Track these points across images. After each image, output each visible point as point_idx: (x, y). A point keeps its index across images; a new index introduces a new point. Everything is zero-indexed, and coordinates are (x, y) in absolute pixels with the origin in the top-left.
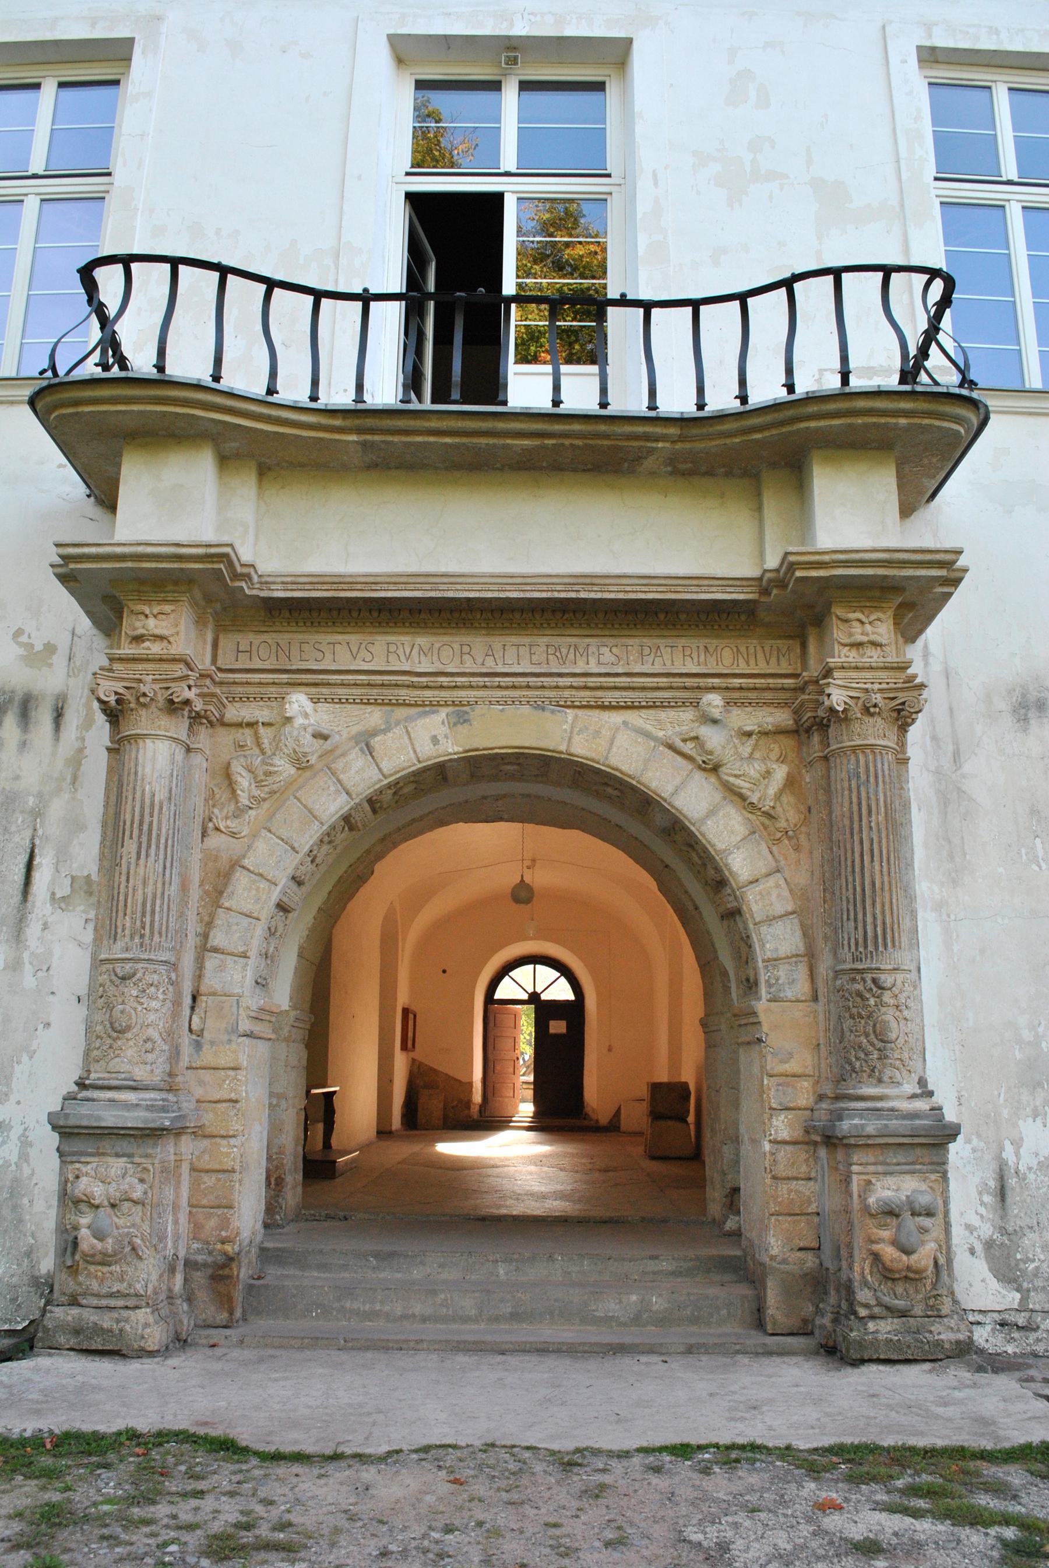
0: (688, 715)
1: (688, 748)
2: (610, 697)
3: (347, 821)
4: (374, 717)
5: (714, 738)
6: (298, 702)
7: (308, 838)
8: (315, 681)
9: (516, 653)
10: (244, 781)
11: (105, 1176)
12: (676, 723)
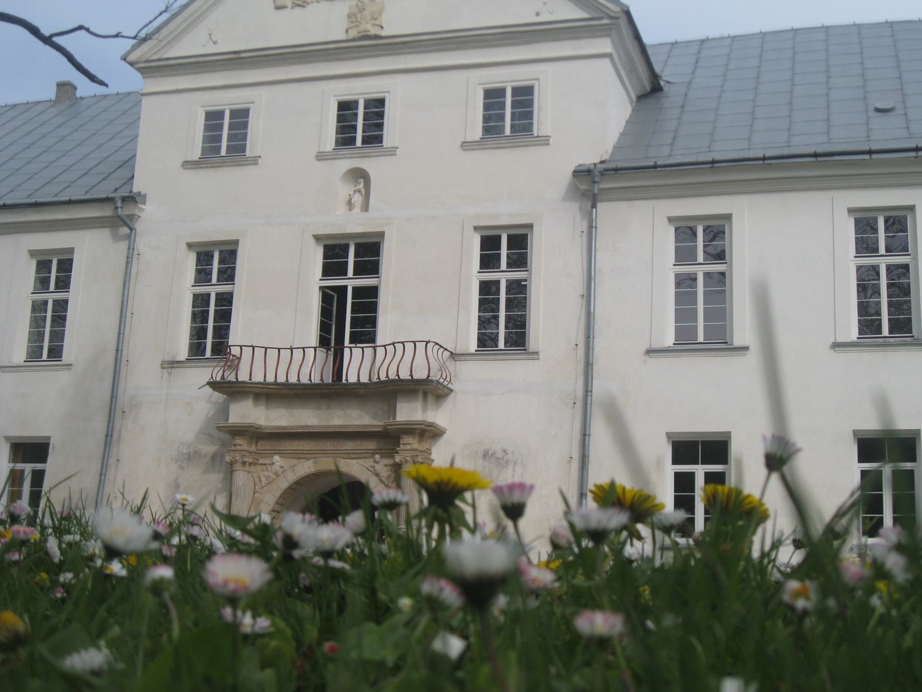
0: (372, 460)
1: (372, 469)
2: (353, 456)
3: (290, 488)
4: (295, 461)
5: (377, 467)
6: (277, 458)
7: (278, 494)
8: (281, 453)
9: (328, 445)
10: (263, 479)
12: (369, 462)
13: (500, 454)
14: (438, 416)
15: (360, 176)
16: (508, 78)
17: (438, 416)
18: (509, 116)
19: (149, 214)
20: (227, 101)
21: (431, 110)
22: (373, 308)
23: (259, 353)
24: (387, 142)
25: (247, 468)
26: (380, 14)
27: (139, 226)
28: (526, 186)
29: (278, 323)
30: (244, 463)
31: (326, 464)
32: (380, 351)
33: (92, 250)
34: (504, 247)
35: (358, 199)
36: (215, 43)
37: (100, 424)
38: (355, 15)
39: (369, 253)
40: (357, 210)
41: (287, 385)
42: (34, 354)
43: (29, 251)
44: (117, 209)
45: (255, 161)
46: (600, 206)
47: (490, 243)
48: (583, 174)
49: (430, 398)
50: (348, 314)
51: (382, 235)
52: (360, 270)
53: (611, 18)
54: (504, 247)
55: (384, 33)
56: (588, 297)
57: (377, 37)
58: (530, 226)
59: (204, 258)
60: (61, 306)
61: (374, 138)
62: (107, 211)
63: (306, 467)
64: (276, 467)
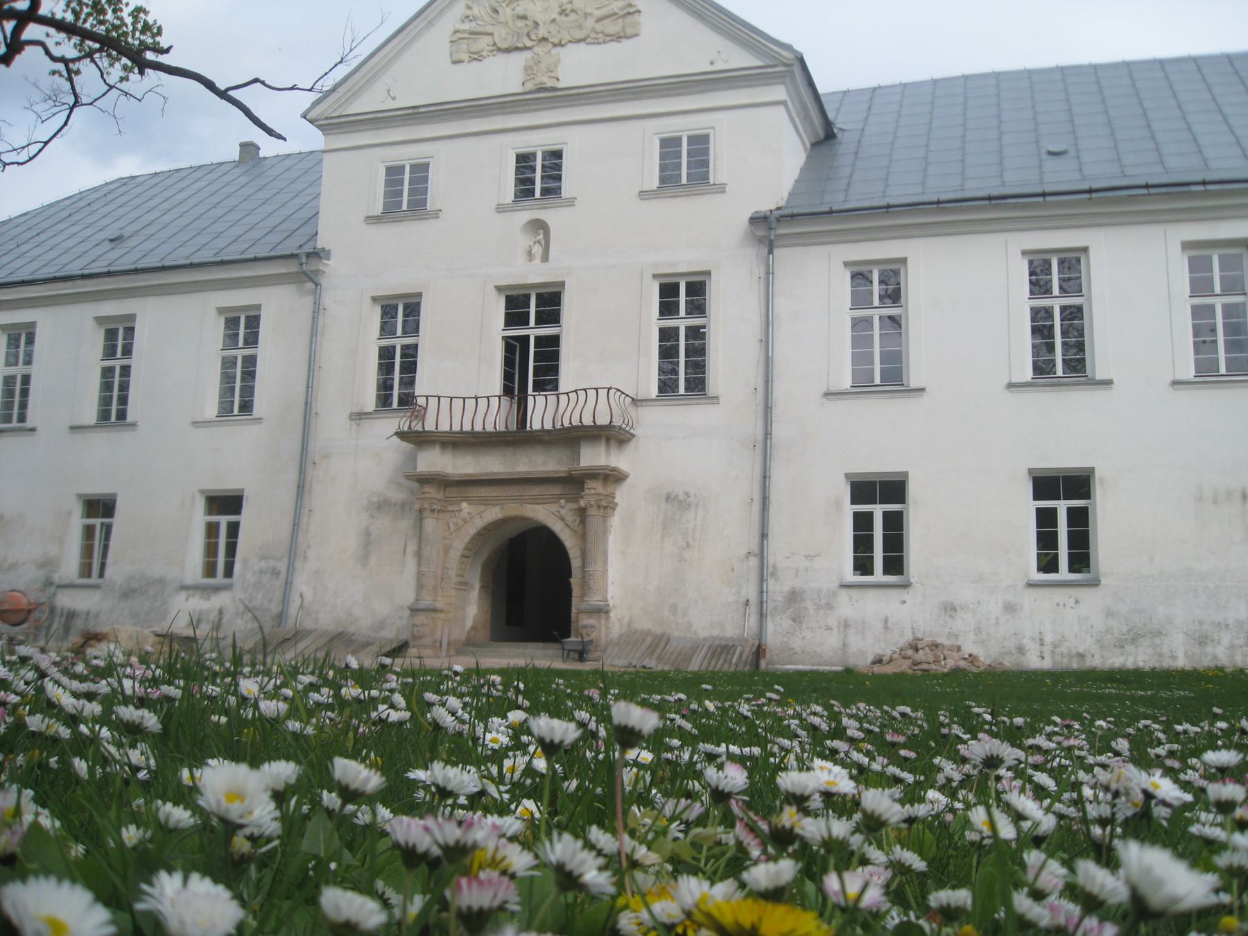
4: (483, 508)
5: (563, 512)
6: (464, 505)
7: (467, 540)
9: (514, 491)
10: (452, 526)
11: (421, 618)
12: (554, 507)
13: (682, 497)
14: (618, 460)
15: (539, 226)
16: (683, 127)
17: (618, 460)
18: (685, 167)
19: (335, 268)
20: (407, 155)
21: (608, 159)
22: (555, 356)
23: (445, 403)
24: (565, 193)
25: (436, 515)
26: (556, 66)
27: (324, 281)
28: (704, 235)
29: (463, 372)
30: (433, 511)
31: (513, 510)
32: (563, 398)
33: (279, 307)
34: (683, 295)
35: (538, 250)
36: (393, 99)
37: (292, 475)
38: (531, 68)
39: (550, 303)
40: (537, 261)
41: (472, 433)
42: (225, 409)
43: (218, 309)
44: (303, 264)
45: (436, 214)
46: (776, 251)
47: (668, 291)
48: (758, 220)
49: (613, 443)
50: (531, 365)
51: (562, 284)
52: (541, 320)
53: (786, 65)
54: (683, 295)
55: (560, 85)
56: (766, 341)
57: (553, 89)
58: (708, 273)
59: (388, 311)
60: (251, 361)
61: (551, 192)
62: (291, 267)
63: (493, 514)
64: (464, 514)
